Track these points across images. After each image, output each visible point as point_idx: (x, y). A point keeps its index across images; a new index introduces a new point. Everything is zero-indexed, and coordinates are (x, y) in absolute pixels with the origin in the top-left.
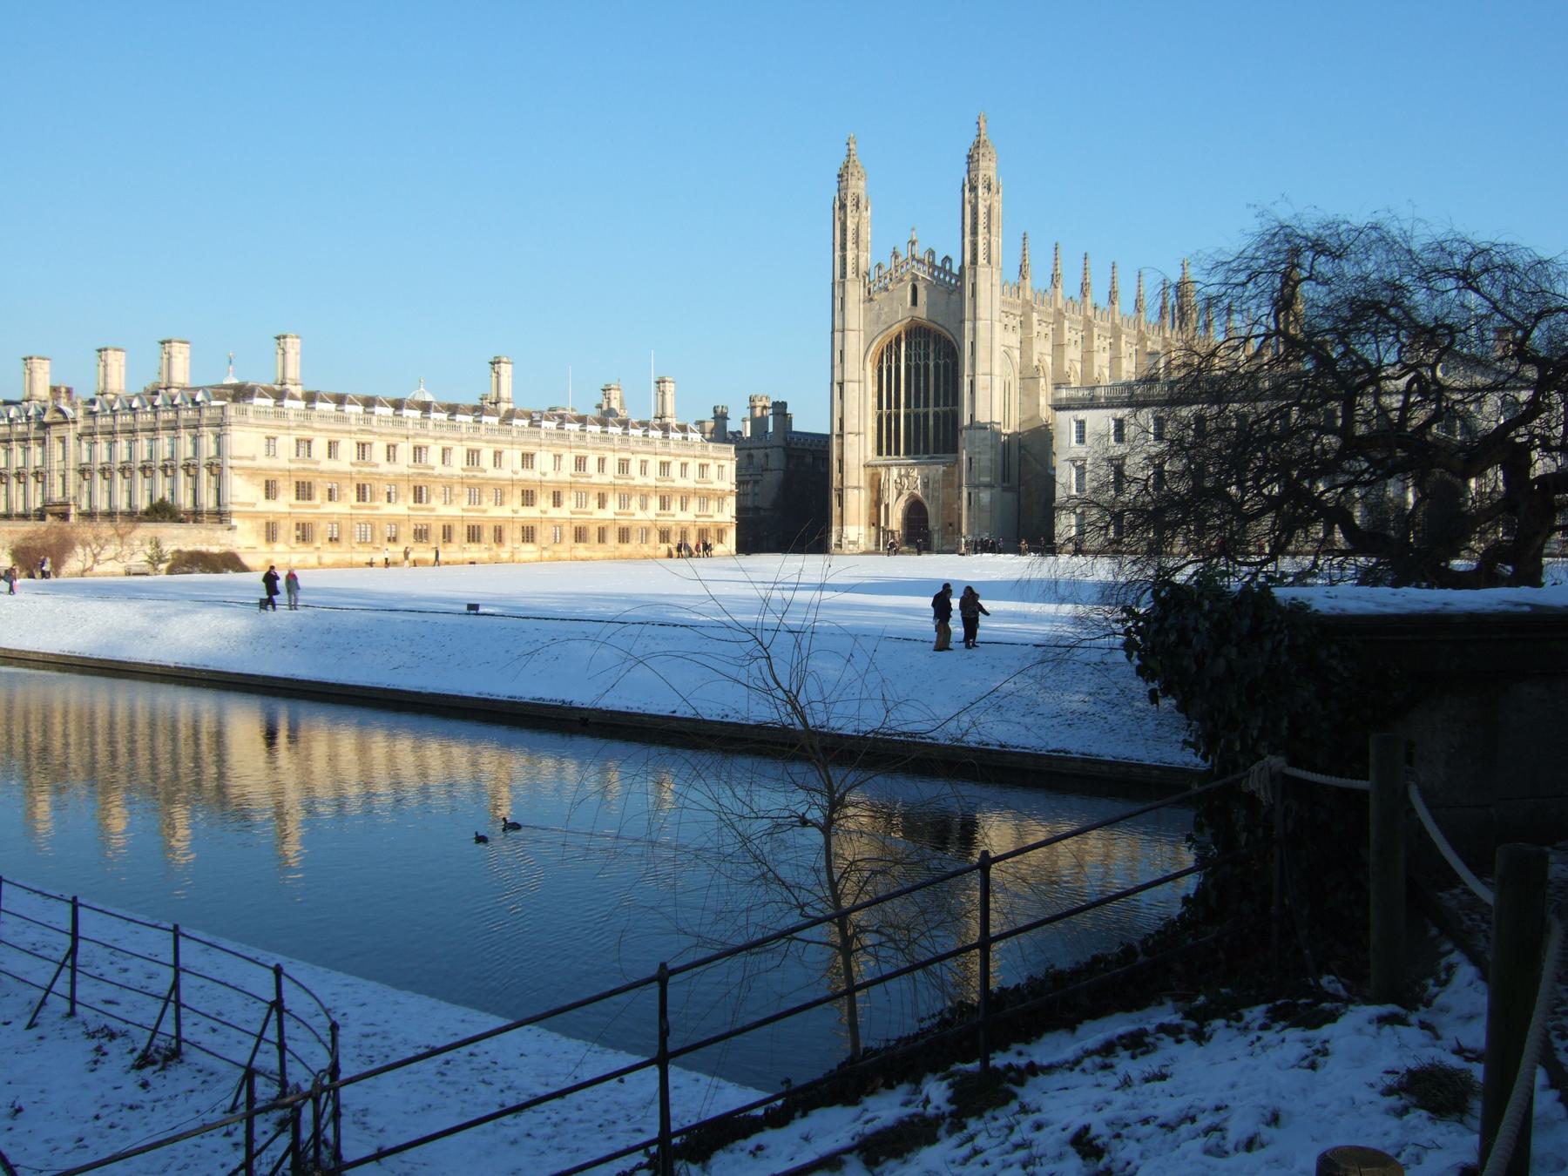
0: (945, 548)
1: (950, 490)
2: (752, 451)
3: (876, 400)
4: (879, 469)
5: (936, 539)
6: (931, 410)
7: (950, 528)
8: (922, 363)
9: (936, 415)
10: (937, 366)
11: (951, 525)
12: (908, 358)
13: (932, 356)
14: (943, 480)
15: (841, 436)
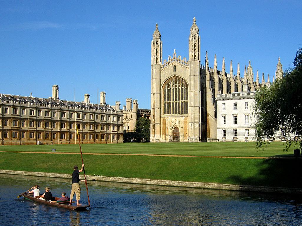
0: (184, 141)
1: (186, 124)
2: (127, 114)
3: (164, 98)
4: (165, 118)
5: (182, 139)
6: (180, 101)
7: (186, 135)
8: (177, 88)
9: (182, 102)
10: (182, 88)
11: (186, 134)
12: (173, 86)
13: (180, 86)
14: (184, 121)
15: (154, 109)
